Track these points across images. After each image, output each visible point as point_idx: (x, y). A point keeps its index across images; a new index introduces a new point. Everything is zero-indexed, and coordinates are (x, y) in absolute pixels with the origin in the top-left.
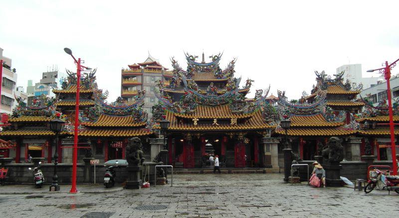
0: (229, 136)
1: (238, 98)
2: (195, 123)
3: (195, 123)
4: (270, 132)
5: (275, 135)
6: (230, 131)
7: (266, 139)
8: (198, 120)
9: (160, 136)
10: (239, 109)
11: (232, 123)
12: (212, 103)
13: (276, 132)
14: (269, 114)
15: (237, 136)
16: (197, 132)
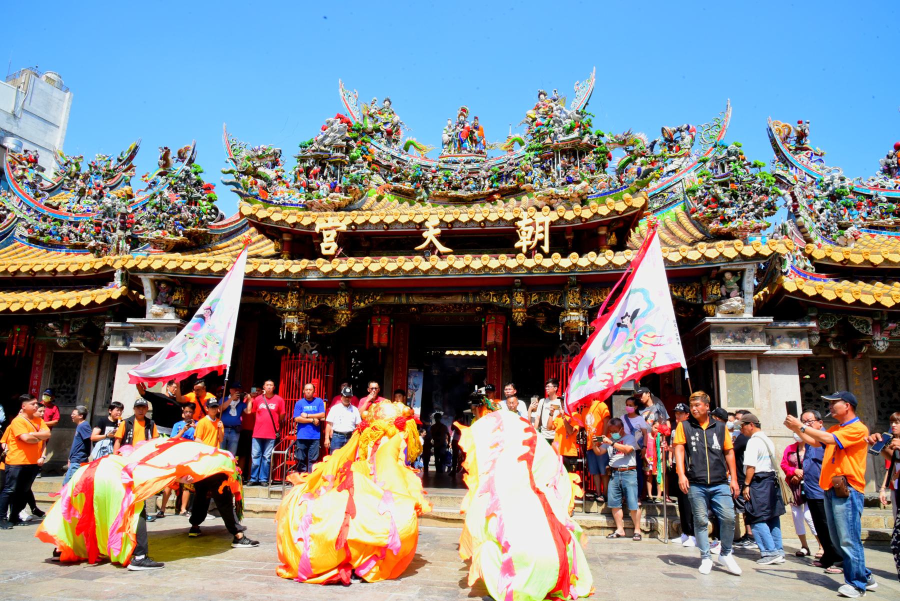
0: (507, 312)
1: (570, 130)
2: (329, 245)
3: (329, 245)
4: (750, 281)
5: (781, 307)
6: (505, 284)
7: (721, 329)
8: (343, 228)
9: (153, 309)
10: (570, 181)
11: (523, 243)
12: (456, 188)
13: (790, 284)
14: (734, 195)
15: (554, 314)
16: (328, 288)
